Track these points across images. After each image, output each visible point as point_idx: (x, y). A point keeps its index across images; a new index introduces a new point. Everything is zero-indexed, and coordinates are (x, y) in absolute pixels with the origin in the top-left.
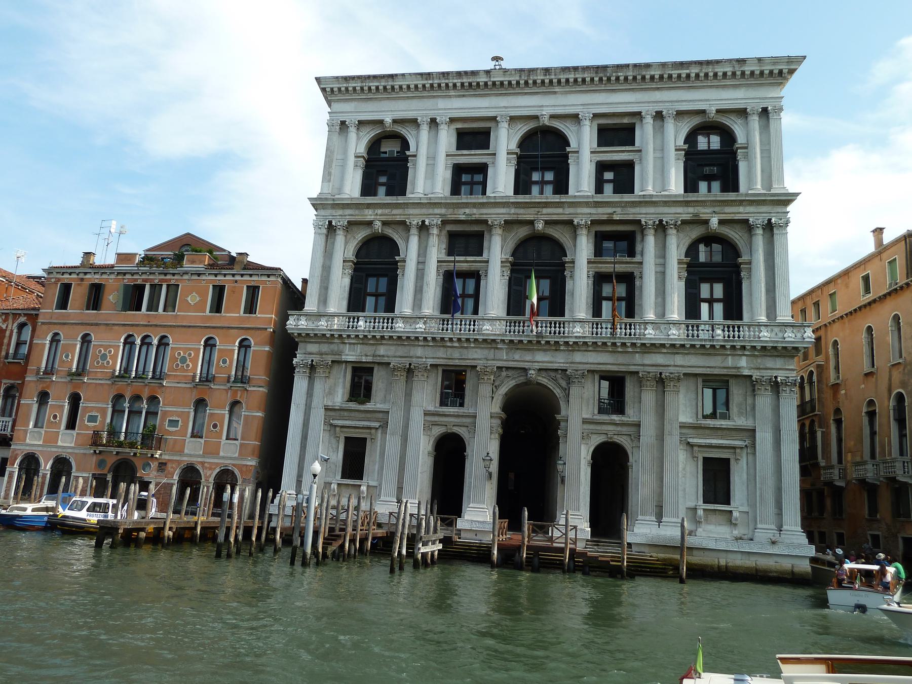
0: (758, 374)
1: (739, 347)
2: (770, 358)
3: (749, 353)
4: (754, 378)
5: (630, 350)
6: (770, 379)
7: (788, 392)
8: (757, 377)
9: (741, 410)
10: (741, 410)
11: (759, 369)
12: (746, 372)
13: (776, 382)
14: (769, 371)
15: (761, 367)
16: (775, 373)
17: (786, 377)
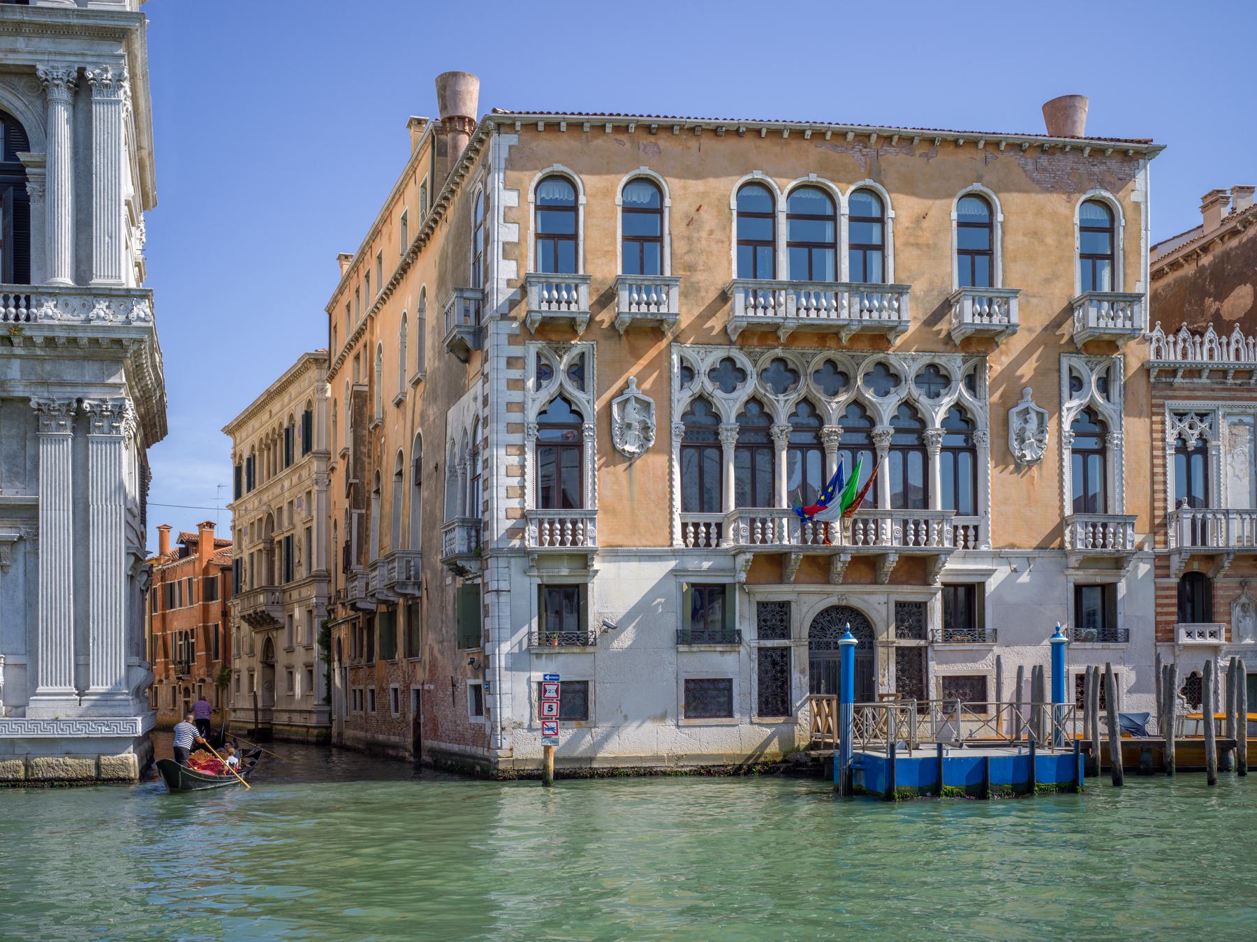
0: (46, 395)
1: (63, 340)
2: (71, 363)
3: (23, 352)
4: (33, 404)
5: (39, 352)
6: (69, 405)
7: (106, 429)
8: (41, 401)
9: (15, 469)
10: (15, 469)
11: (44, 383)
12: (19, 391)
13: (80, 413)
14: (69, 389)
15: (52, 380)
16: (78, 392)
17: (100, 400)
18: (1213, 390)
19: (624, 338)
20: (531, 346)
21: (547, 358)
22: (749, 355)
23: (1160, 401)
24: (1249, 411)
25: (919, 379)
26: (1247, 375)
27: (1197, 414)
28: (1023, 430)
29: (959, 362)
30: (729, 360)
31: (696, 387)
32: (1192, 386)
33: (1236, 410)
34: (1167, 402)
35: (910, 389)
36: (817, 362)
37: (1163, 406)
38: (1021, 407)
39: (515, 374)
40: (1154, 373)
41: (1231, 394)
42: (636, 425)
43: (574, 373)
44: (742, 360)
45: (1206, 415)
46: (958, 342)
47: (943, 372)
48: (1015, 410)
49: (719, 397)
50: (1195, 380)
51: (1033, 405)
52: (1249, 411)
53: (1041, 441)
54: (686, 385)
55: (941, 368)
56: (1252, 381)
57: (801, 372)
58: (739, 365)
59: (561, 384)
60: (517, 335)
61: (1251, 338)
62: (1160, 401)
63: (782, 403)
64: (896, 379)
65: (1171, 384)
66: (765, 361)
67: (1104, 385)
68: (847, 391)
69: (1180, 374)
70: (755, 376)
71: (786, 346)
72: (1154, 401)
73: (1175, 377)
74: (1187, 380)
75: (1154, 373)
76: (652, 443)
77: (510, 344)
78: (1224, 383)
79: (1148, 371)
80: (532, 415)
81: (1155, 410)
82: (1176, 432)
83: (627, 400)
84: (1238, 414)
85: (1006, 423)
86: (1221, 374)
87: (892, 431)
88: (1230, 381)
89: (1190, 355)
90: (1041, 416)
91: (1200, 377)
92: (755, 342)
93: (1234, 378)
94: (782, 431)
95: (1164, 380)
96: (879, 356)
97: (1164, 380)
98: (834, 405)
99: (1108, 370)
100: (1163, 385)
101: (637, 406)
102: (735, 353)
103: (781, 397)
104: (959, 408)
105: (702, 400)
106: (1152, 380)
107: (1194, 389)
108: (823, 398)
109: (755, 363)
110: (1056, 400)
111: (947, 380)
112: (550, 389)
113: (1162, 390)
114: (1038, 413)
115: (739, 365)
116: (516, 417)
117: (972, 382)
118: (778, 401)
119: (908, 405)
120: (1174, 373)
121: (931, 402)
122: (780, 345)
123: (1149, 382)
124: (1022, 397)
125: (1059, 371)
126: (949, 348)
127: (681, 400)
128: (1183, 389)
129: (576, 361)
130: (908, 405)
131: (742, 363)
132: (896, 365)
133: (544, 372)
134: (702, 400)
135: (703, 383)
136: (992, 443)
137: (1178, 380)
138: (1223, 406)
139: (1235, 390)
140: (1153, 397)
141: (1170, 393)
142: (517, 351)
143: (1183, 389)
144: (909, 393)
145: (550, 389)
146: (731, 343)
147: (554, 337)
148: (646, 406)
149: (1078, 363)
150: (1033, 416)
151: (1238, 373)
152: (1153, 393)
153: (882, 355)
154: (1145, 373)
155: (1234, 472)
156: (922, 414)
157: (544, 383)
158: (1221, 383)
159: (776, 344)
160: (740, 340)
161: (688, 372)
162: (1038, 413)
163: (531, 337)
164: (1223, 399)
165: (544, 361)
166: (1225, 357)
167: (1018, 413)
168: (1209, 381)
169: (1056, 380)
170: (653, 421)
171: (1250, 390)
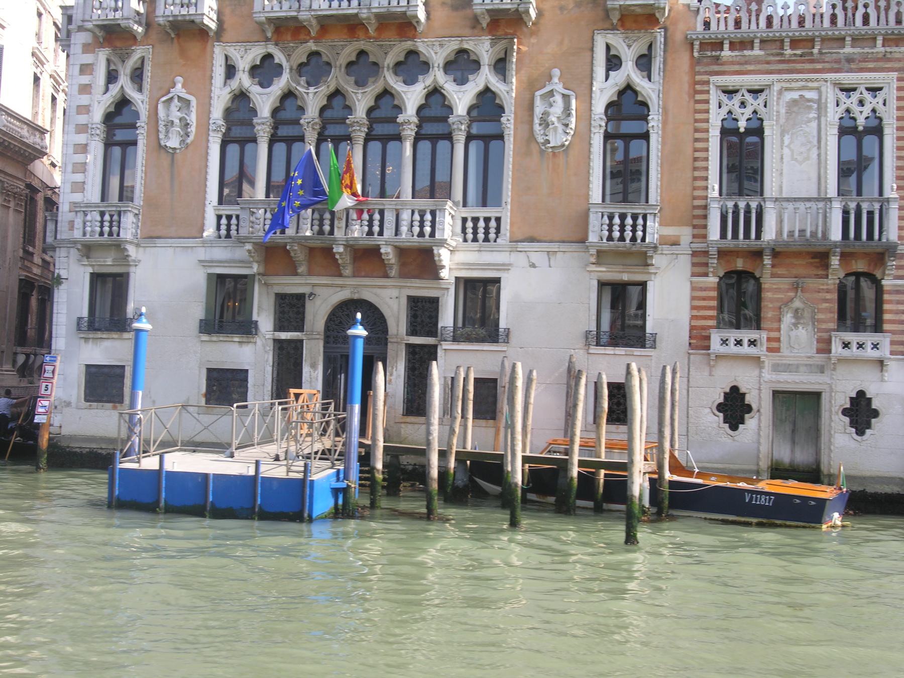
18: (768, 63)
19: (175, 41)
20: (100, 53)
21: (115, 64)
22: (283, 50)
23: (705, 78)
24: (810, 84)
25: (448, 66)
26: (810, 44)
27: (750, 91)
28: (546, 114)
29: (487, 45)
30: (268, 57)
31: (234, 84)
32: (743, 59)
33: (794, 85)
34: (713, 79)
35: (438, 76)
36: (348, 52)
37: (707, 83)
38: (548, 89)
39: (85, 79)
40: (696, 47)
41: (788, 66)
42: (177, 121)
43: (137, 76)
44: (279, 57)
45: (761, 91)
46: (485, 25)
47: (473, 57)
48: (538, 93)
49: (255, 91)
50: (746, 53)
51: (559, 88)
52: (810, 84)
53: (567, 125)
54: (228, 81)
55: (471, 54)
56: (815, 51)
57: (333, 64)
58: (277, 61)
59: (122, 87)
60: (90, 44)
61: (754, 4)
62: (705, 78)
63: (311, 95)
64: (426, 66)
65: (717, 58)
66: (301, 55)
67: (644, 62)
68: (374, 82)
69: (726, 46)
70: (288, 71)
71: (317, 40)
72: (698, 78)
73: (722, 50)
74: (736, 53)
75: (696, 47)
76: (192, 138)
77: (83, 53)
78: (782, 54)
79: (692, 45)
80: (98, 115)
81: (698, 87)
82: (723, 112)
83: (172, 98)
84: (799, 89)
85: (531, 107)
86: (778, 44)
87: (415, 120)
88: (788, 52)
89: (744, 25)
90: (566, 98)
91: (752, 49)
92: (289, 38)
93: (792, 48)
94: (308, 123)
95: (709, 54)
96: (408, 45)
97: (709, 54)
98: (360, 96)
99: (650, 46)
100: (709, 60)
101: (179, 104)
102: (272, 49)
103: (312, 90)
104: (486, 93)
105: (241, 97)
106: (696, 54)
107: (746, 63)
108: (350, 89)
109: (288, 57)
110: (588, 81)
111: (476, 65)
112: (115, 89)
113: (708, 64)
114: (564, 95)
115: (277, 61)
116: (82, 119)
117: (501, 66)
118: (307, 93)
119: (435, 92)
120: (719, 45)
121: (457, 88)
122: (312, 38)
123: (692, 56)
124: (550, 78)
125: (592, 50)
126: (476, 31)
127: (221, 97)
128: (733, 63)
129: (138, 65)
130: (435, 92)
131: (279, 58)
132: (424, 52)
133: (112, 77)
134: (241, 97)
135: (244, 80)
136: (516, 129)
137: (726, 53)
138: (779, 81)
139: (794, 62)
140: (700, 73)
141: (716, 68)
142: (88, 59)
143: (733, 63)
144: (435, 80)
145: (115, 89)
146: (267, 40)
147: (118, 44)
148: (187, 103)
149: (617, 41)
150: (558, 99)
151: (795, 43)
152: (698, 69)
153: (410, 43)
154: (688, 47)
155: (792, 155)
156: (449, 101)
157: (111, 86)
158: (778, 55)
159: (308, 38)
160: (275, 37)
161: (230, 71)
162: (564, 95)
163: (101, 46)
164: (779, 72)
165: (112, 67)
166: (753, 26)
167: (543, 97)
168: (762, 53)
169: (589, 59)
170: (193, 118)
171: (812, 61)
